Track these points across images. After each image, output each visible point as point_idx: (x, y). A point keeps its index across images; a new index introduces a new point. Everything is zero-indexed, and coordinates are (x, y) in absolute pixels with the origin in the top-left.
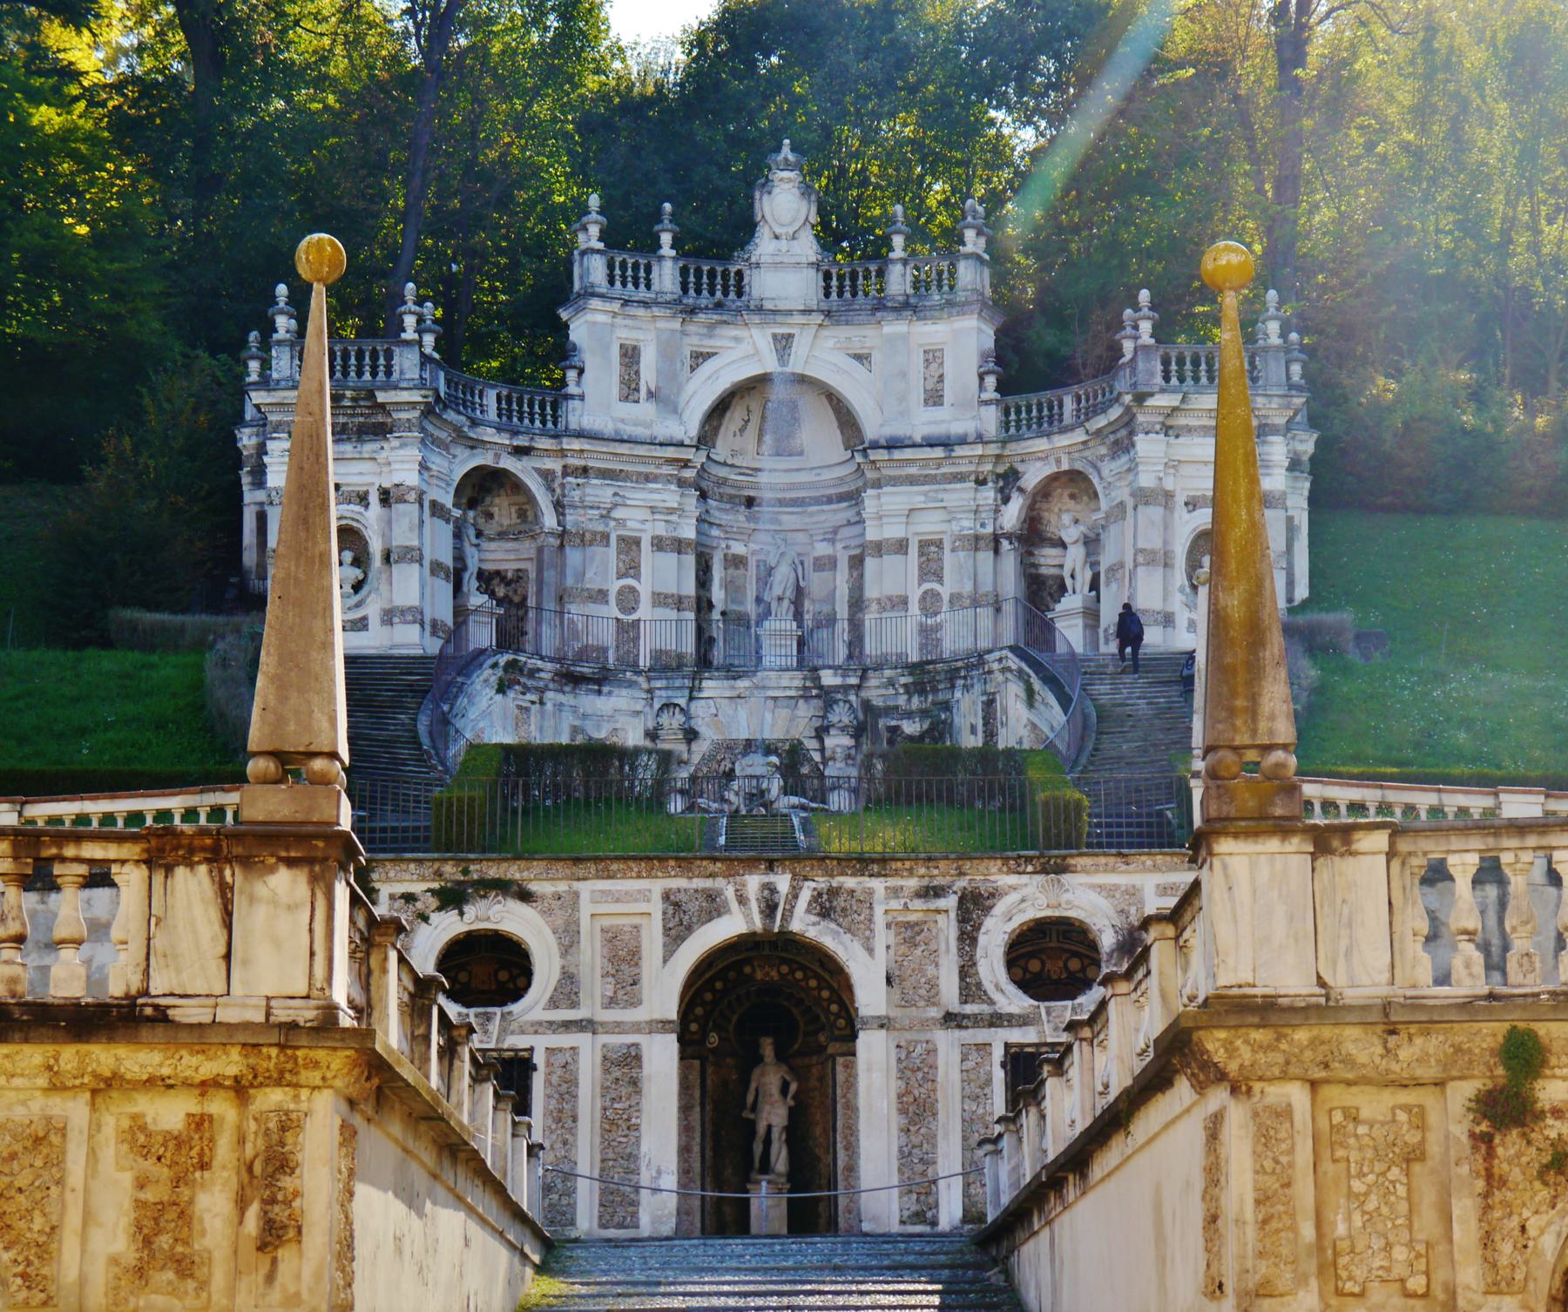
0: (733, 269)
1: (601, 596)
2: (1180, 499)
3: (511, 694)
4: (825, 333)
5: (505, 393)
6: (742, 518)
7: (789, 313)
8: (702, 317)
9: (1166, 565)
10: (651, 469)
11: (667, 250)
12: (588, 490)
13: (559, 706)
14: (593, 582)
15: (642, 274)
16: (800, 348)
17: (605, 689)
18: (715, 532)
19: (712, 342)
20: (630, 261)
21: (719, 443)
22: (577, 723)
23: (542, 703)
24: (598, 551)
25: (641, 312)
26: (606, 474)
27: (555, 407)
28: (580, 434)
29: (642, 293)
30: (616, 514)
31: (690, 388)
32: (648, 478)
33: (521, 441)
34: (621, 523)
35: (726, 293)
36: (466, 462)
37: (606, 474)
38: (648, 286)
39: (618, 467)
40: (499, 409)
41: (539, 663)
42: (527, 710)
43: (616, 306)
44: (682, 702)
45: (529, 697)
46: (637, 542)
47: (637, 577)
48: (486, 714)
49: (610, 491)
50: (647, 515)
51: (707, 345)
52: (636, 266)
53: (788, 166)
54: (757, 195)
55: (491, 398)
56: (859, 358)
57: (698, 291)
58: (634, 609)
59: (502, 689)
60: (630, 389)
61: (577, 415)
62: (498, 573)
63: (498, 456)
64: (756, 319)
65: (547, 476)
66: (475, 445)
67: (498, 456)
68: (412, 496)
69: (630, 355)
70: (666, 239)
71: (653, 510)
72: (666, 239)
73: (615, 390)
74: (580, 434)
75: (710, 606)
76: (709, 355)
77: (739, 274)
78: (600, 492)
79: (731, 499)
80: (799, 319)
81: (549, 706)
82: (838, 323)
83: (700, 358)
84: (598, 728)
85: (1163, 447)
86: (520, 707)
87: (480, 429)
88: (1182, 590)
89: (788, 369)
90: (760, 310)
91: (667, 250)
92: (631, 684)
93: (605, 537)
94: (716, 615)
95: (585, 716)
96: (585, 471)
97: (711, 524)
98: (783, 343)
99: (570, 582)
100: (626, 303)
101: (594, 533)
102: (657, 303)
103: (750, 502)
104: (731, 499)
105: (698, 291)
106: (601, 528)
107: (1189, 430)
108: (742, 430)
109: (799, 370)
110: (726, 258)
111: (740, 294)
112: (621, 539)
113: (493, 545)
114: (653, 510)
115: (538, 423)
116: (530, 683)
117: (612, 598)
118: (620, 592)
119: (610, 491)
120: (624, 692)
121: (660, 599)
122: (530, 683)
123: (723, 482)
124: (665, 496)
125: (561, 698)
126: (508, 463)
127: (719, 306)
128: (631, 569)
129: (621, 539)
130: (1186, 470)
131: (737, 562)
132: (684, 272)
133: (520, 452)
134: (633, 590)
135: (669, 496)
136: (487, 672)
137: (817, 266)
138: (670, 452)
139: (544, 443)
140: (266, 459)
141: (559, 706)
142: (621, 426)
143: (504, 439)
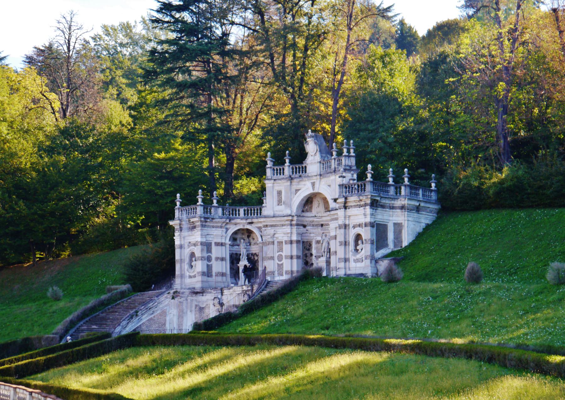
0: (304, 166)
1: (272, 258)
2: (351, 226)
3: (176, 299)
4: (323, 180)
5: (246, 209)
6: (319, 230)
7: (312, 176)
8: (295, 180)
9: (345, 244)
10: (283, 223)
11: (287, 163)
12: (267, 231)
13: (192, 300)
14: (270, 254)
15: (282, 171)
16: (317, 185)
17: (204, 294)
18: (312, 235)
19: (300, 186)
20: (278, 168)
21: (313, 210)
22: (197, 304)
23: (187, 300)
24: (271, 246)
25: (280, 182)
26: (272, 226)
27: (261, 210)
28: (265, 217)
29: (282, 176)
30: (276, 236)
31: (294, 199)
32: (283, 225)
33: (249, 221)
34: (277, 238)
35: (303, 172)
36: (233, 229)
37: (272, 226)
38: (283, 174)
39: (275, 224)
40: (245, 213)
41: (184, 291)
42: (182, 302)
43: (272, 181)
44: (220, 296)
45: (182, 299)
46: (282, 242)
47: (282, 251)
48: (166, 306)
49: (273, 230)
50: (282, 235)
51: (298, 187)
52: (280, 169)
53: (311, 137)
54: (305, 145)
55: (242, 211)
56: (329, 186)
57: (296, 173)
58: (281, 261)
59: (173, 298)
60: (280, 202)
61: (265, 212)
62: (255, 254)
63: (244, 226)
64: (306, 179)
65: (259, 228)
66: (236, 224)
67: (244, 226)
68: (199, 244)
69: (279, 193)
70: (287, 161)
71: (284, 234)
72: (287, 161)
73: (276, 202)
74: (265, 217)
75: (311, 255)
76: (299, 190)
77: (306, 167)
78: (270, 231)
79: (317, 225)
80: (315, 178)
81: (189, 301)
82: (324, 177)
83: (297, 191)
84: (203, 304)
85: (343, 212)
86: (180, 302)
87: (235, 220)
88: (351, 251)
89: (315, 191)
90: (308, 176)
91: (287, 163)
92: (210, 293)
93: (273, 243)
94: (314, 257)
95: (199, 302)
96: (267, 226)
97: (310, 233)
98: (313, 184)
99: (264, 255)
100: (275, 180)
101: (269, 242)
102: (283, 179)
103: (322, 225)
104: (317, 225)
105: (296, 173)
106: (271, 240)
107: (351, 206)
108: (318, 206)
109: (317, 191)
110: (302, 163)
111: (306, 172)
112: (278, 242)
113: (254, 247)
114: (284, 234)
115: (256, 215)
116: (182, 295)
117: (276, 258)
118: (278, 256)
119: (273, 230)
120: (209, 294)
121: (286, 257)
122: (182, 295)
123: (313, 221)
124: (287, 230)
125: (192, 298)
126: (249, 227)
127: (300, 176)
128: (281, 250)
129: (278, 242)
130: (352, 218)
131: (318, 242)
132: (293, 169)
133: (251, 223)
134: (281, 255)
135: (288, 229)
136: (165, 296)
137: (320, 162)
138: (286, 218)
139: (255, 220)
140: (174, 238)
141: (192, 300)
142: (276, 213)
143: (244, 221)
